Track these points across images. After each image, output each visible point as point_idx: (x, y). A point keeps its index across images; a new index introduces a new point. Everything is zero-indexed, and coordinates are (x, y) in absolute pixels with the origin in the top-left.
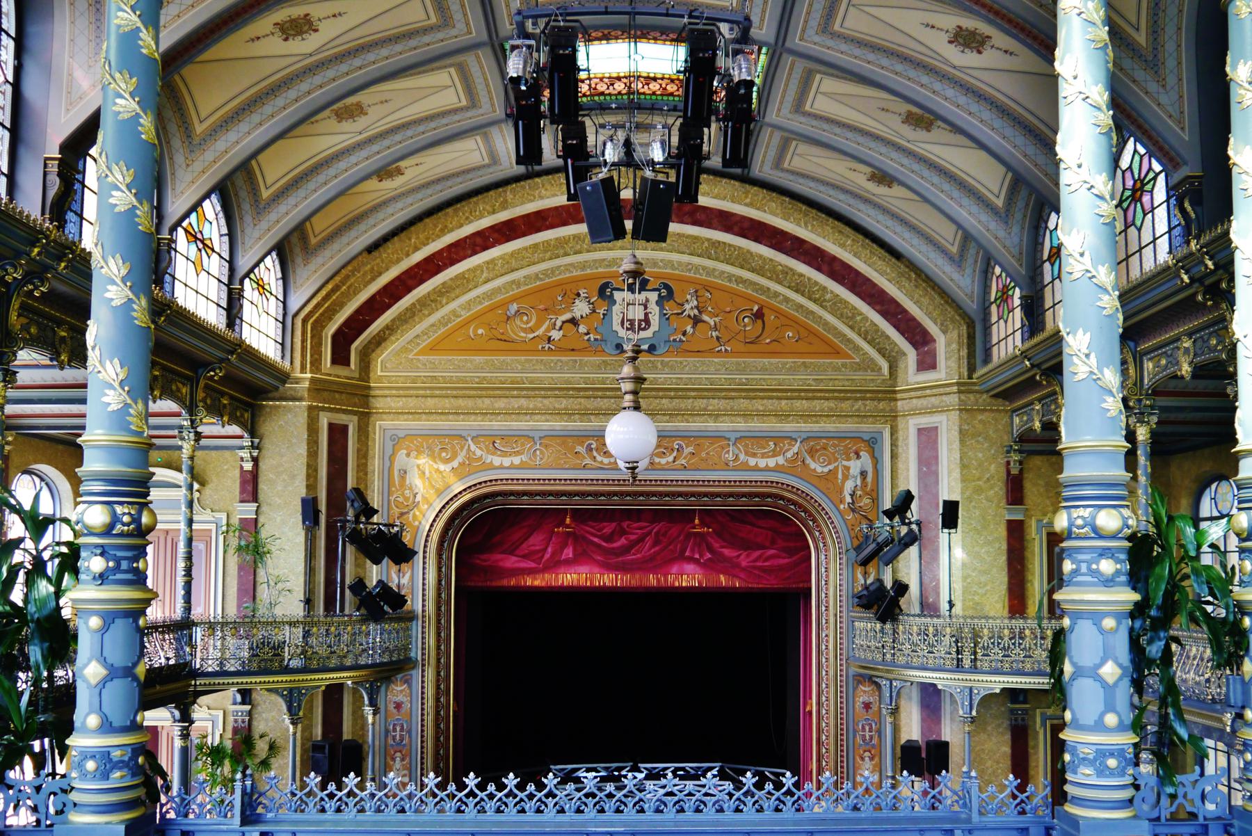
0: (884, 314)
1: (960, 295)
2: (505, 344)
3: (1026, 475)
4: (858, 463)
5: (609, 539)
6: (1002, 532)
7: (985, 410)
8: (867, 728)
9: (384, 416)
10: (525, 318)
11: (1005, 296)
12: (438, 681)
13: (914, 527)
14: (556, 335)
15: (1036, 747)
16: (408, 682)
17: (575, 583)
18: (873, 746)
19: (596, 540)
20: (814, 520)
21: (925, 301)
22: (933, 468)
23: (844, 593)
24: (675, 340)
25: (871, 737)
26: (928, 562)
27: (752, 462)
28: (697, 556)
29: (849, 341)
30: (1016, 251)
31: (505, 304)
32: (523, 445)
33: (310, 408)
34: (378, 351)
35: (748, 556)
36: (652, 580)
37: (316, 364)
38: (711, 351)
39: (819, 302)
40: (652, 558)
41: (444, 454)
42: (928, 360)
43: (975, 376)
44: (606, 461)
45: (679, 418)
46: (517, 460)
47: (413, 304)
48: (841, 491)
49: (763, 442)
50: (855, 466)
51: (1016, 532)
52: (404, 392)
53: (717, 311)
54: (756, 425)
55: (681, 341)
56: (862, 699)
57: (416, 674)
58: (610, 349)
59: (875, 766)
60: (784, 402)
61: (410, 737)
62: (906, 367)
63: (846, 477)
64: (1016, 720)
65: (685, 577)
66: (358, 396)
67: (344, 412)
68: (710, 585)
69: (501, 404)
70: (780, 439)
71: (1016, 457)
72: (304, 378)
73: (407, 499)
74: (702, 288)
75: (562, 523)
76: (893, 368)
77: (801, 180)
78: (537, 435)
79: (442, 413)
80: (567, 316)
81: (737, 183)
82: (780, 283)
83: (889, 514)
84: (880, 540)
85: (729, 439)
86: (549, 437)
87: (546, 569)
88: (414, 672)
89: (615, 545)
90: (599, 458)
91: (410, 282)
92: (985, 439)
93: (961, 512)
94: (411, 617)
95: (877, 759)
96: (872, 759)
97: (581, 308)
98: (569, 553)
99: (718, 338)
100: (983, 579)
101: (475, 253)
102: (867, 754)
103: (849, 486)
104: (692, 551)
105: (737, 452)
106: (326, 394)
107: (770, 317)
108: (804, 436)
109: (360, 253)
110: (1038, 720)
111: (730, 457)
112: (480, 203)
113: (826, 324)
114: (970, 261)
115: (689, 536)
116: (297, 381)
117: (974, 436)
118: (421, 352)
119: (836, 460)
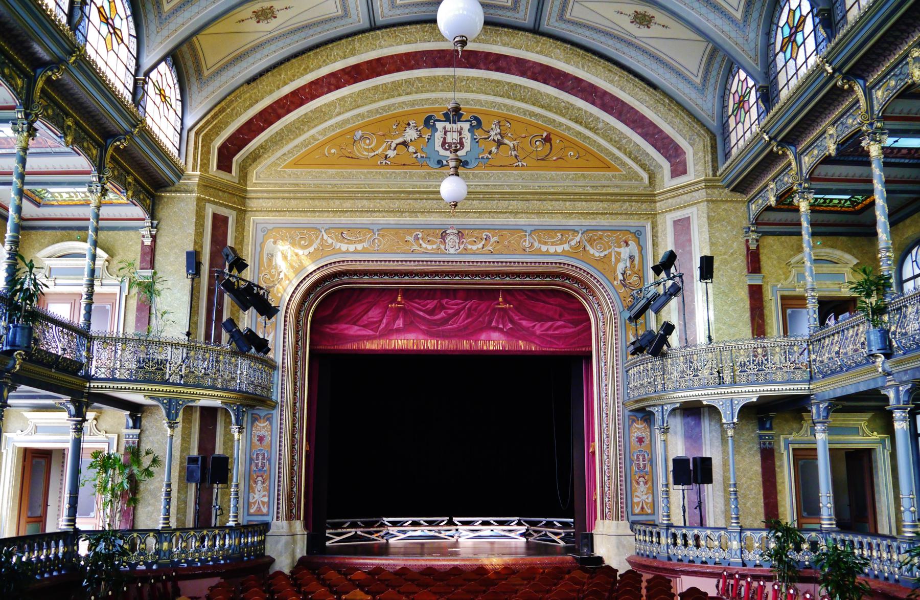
0: (644, 136)
1: (703, 115)
2: (352, 160)
3: (761, 251)
4: (627, 249)
5: (431, 312)
6: (744, 294)
7: (727, 201)
8: (641, 458)
9: (257, 213)
10: (368, 141)
11: (742, 102)
12: (294, 420)
13: (677, 280)
14: (391, 154)
15: (782, 466)
16: (269, 419)
17: (405, 347)
18: (646, 473)
19: (421, 313)
20: (594, 295)
21: (677, 120)
22: (688, 249)
23: (619, 345)
24: (483, 158)
25: (645, 466)
26: (685, 311)
27: (544, 248)
28: (501, 326)
29: (617, 158)
30: (752, 54)
31: (353, 131)
32: (364, 235)
33: (199, 199)
34: (254, 165)
35: (541, 326)
36: (465, 345)
37: (205, 166)
38: (510, 166)
39: (594, 130)
40: (466, 327)
41: (303, 242)
42: (681, 168)
43: (718, 174)
44: (429, 247)
45: (487, 215)
46: (360, 247)
47: (282, 129)
48: (615, 272)
49: (553, 234)
50: (625, 252)
51: (756, 293)
52: (273, 195)
53: (515, 137)
54: (547, 221)
55: (487, 158)
56: (636, 434)
57: (276, 413)
58: (433, 164)
59: (648, 489)
60: (568, 203)
61: (270, 464)
62: (663, 177)
63: (618, 260)
64: (764, 444)
65: (492, 342)
66: (238, 196)
67: (226, 206)
68: (512, 348)
69: (348, 204)
70: (565, 231)
71: (754, 236)
72: (193, 175)
73: (273, 276)
74: (504, 120)
75: (394, 300)
76: (652, 177)
77: (580, 30)
78: (375, 228)
79: (301, 211)
80: (400, 140)
81: (530, 35)
82: (563, 116)
83: (657, 270)
84: (649, 296)
85: (526, 231)
86: (384, 230)
87: (380, 337)
88: (274, 412)
89: (436, 317)
90: (424, 245)
91: (280, 111)
92: (728, 223)
93: (716, 265)
94: (272, 366)
95: (650, 483)
96: (646, 483)
97: (410, 134)
98: (400, 323)
99: (516, 156)
100: (732, 331)
101: (330, 91)
102: (642, 479)
103: (620, 267)
104: (498, 322)
105: (532, 241)
106: (212, 191)
107: (556, 141)
109: (242, 85)
110: (782, 444)
111: (527, 244)
112: (335, 50)
113: (599, 146)
114: (711, 89)
115: (494, 310)
116: (189, 177)
117: (719, 221)
118: (286, 167)
119: (610, 247)
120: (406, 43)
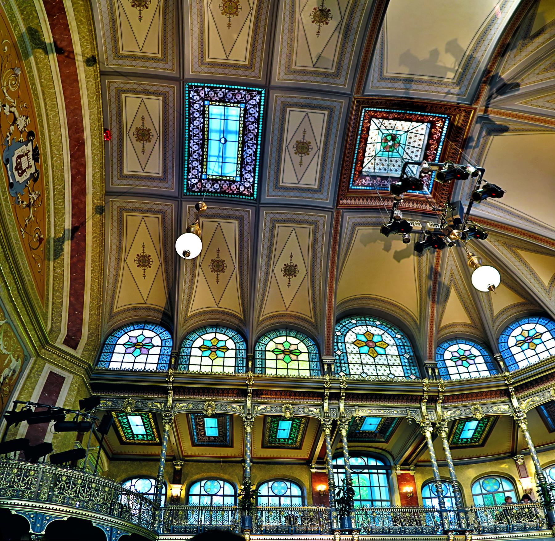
10: (14, 82)
29: (48, 298)
38: (20, 225)
97: (21, 122)
99: (26, 225)
108: (10, 321)
119: (9, 351)
120: (89, 101)
